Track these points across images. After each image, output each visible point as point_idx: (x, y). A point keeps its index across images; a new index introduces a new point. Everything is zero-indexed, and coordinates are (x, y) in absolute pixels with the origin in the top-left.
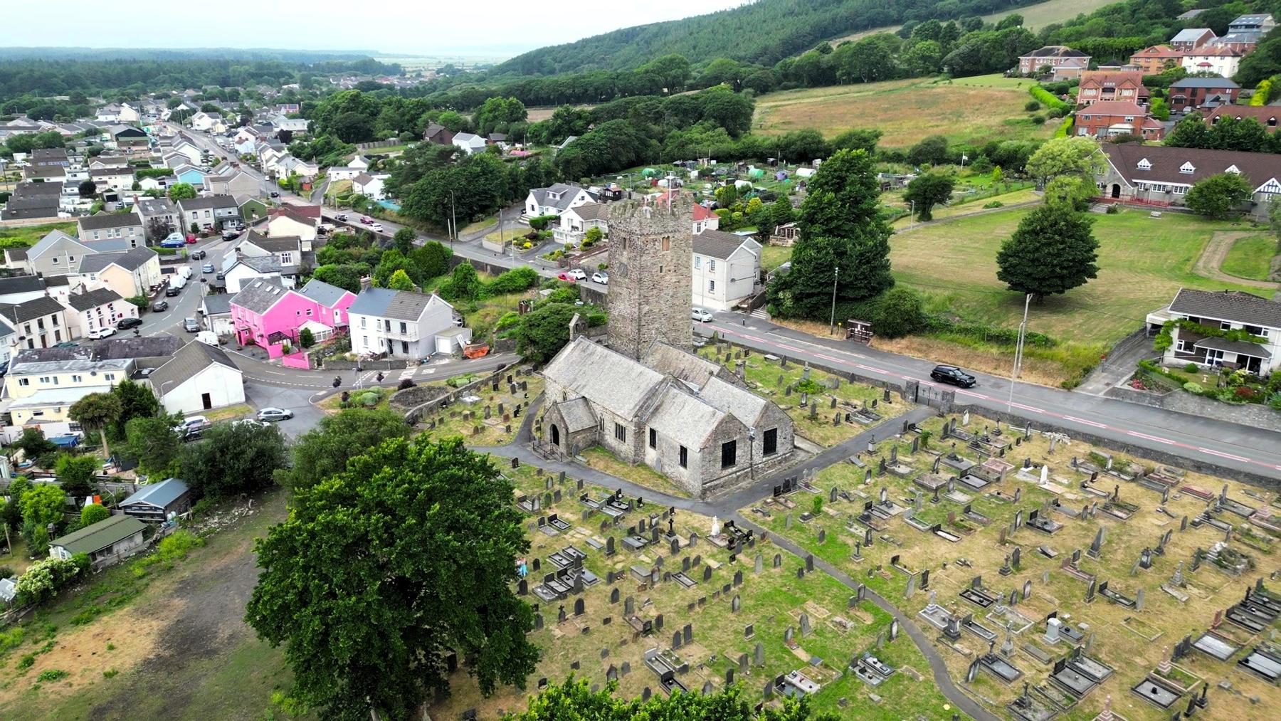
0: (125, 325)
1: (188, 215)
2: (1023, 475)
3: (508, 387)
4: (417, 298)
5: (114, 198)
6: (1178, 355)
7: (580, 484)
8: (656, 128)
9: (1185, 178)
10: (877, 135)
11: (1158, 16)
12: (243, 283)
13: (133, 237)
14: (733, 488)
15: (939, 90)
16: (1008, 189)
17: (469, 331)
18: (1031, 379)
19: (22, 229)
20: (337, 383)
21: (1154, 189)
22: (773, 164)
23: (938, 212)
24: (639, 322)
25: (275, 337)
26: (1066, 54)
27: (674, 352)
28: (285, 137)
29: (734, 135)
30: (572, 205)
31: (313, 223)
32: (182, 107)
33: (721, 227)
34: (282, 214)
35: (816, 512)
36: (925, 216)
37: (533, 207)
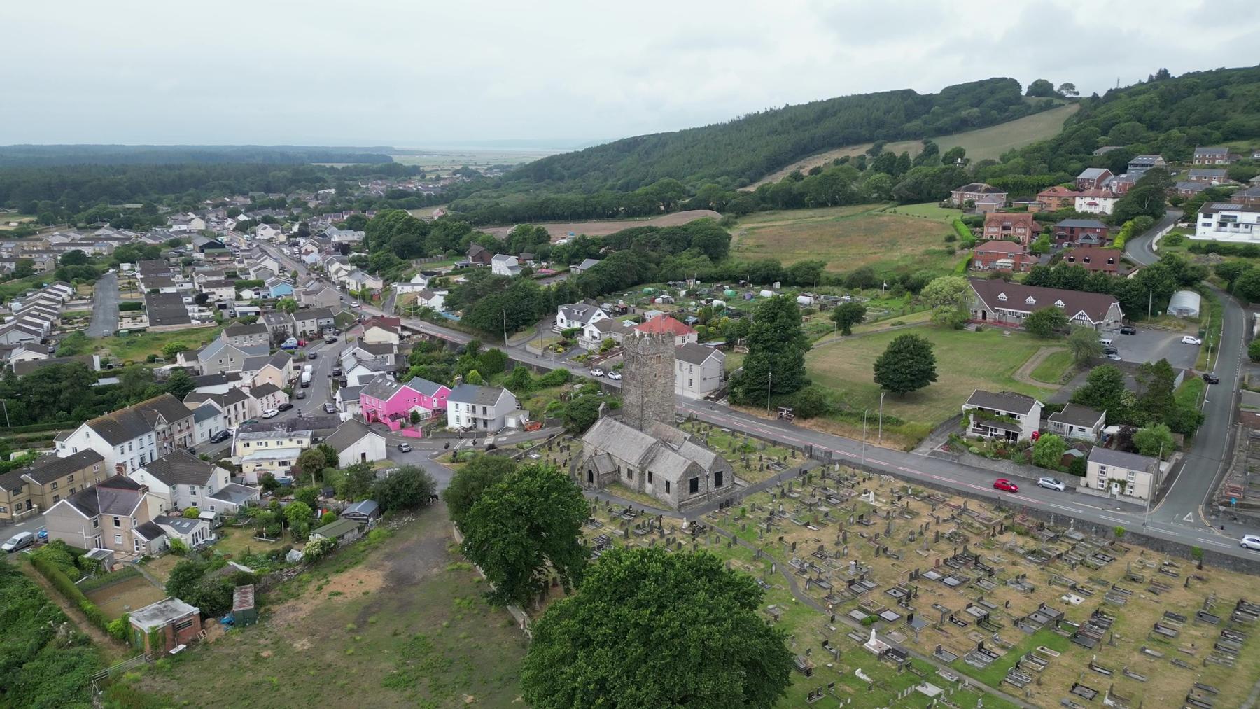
0: (284, 409)
1: (299, 324)
2: (863, 498)
3: (558, 449)
5: (224, 307)
6: (974, 430)
7: (608, 503)
8: (654, 255)
9: (1029, 307)
10: (823, 265)
11: (1076, 152)
12: (361, 378)
15: (885, 219)
16: (913, 311)
17: (527, 413)
18: (887, 445)
19: (168, 333)
20: (447, 446)
21: (1010, 314)
22: (743, 285)
23: (856, 329)
24: (642, 407)
25: (394, 417)
26: (987, 191)
27: (663, 426)
28: (344, 249)
29: (715, 258)
30: (591, 321)
31: (395, 331)
32: (242, 218)
33: (700, 339)
34: (374, 325)
35: (743, 516)
36: (847, 332)
37: (562, 321)
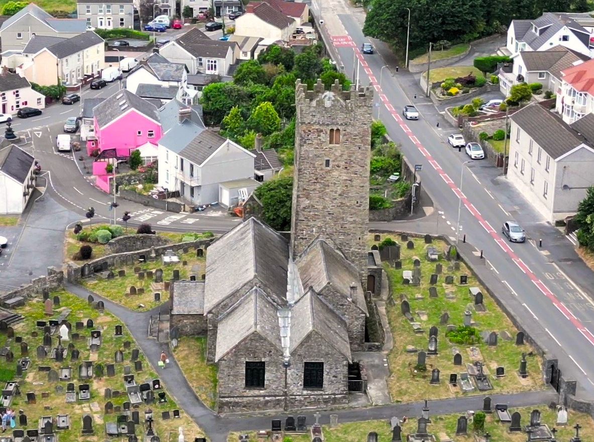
4: (216, 139)
14: (257, 411)
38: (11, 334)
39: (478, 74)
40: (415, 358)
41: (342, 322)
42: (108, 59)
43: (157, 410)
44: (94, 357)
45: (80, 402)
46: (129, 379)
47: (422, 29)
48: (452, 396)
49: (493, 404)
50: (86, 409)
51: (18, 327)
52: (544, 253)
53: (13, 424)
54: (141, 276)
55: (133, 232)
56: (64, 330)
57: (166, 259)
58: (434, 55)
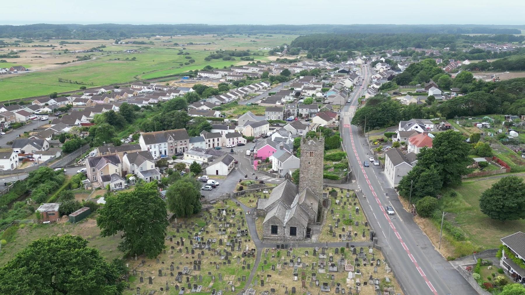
1: (300, 110)
13: (279, 115)
34: (317, 115)
38: (209, 212)
39: (385, 138)
40: (329, 228)
41: (307, 215)
42: (270, 129)
43: (243, 239)
44: (231, 221)
45: (222, 235)
46: (239, 229)
47: (370, 123)
48: (338, 241)
49: (349, 245)
50: (222, 237)
51: (212, 210)
52: (387, 197)
53: (199, 240)
54: (255, 197)
55: (258, 183)
56: (224, 211)
57: (264, 192)
58: (373, 132)
